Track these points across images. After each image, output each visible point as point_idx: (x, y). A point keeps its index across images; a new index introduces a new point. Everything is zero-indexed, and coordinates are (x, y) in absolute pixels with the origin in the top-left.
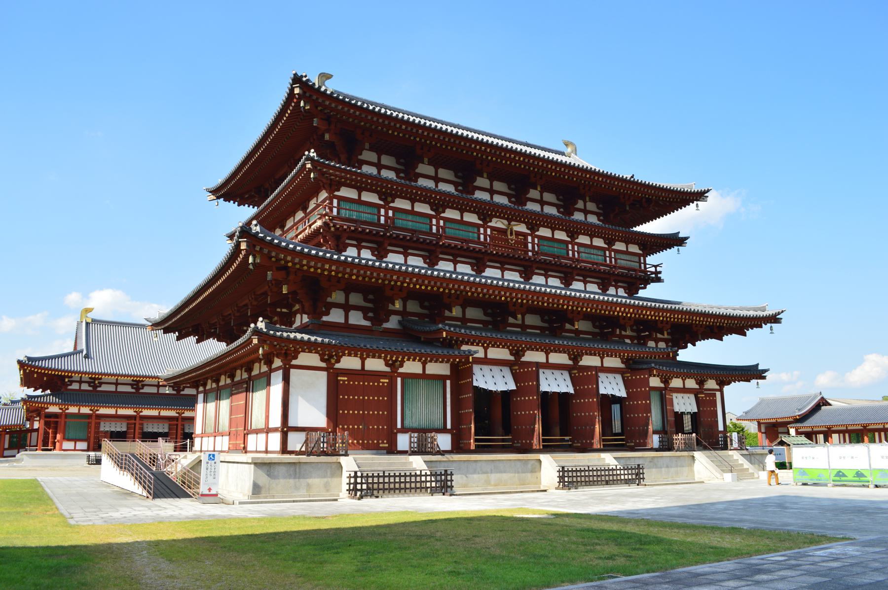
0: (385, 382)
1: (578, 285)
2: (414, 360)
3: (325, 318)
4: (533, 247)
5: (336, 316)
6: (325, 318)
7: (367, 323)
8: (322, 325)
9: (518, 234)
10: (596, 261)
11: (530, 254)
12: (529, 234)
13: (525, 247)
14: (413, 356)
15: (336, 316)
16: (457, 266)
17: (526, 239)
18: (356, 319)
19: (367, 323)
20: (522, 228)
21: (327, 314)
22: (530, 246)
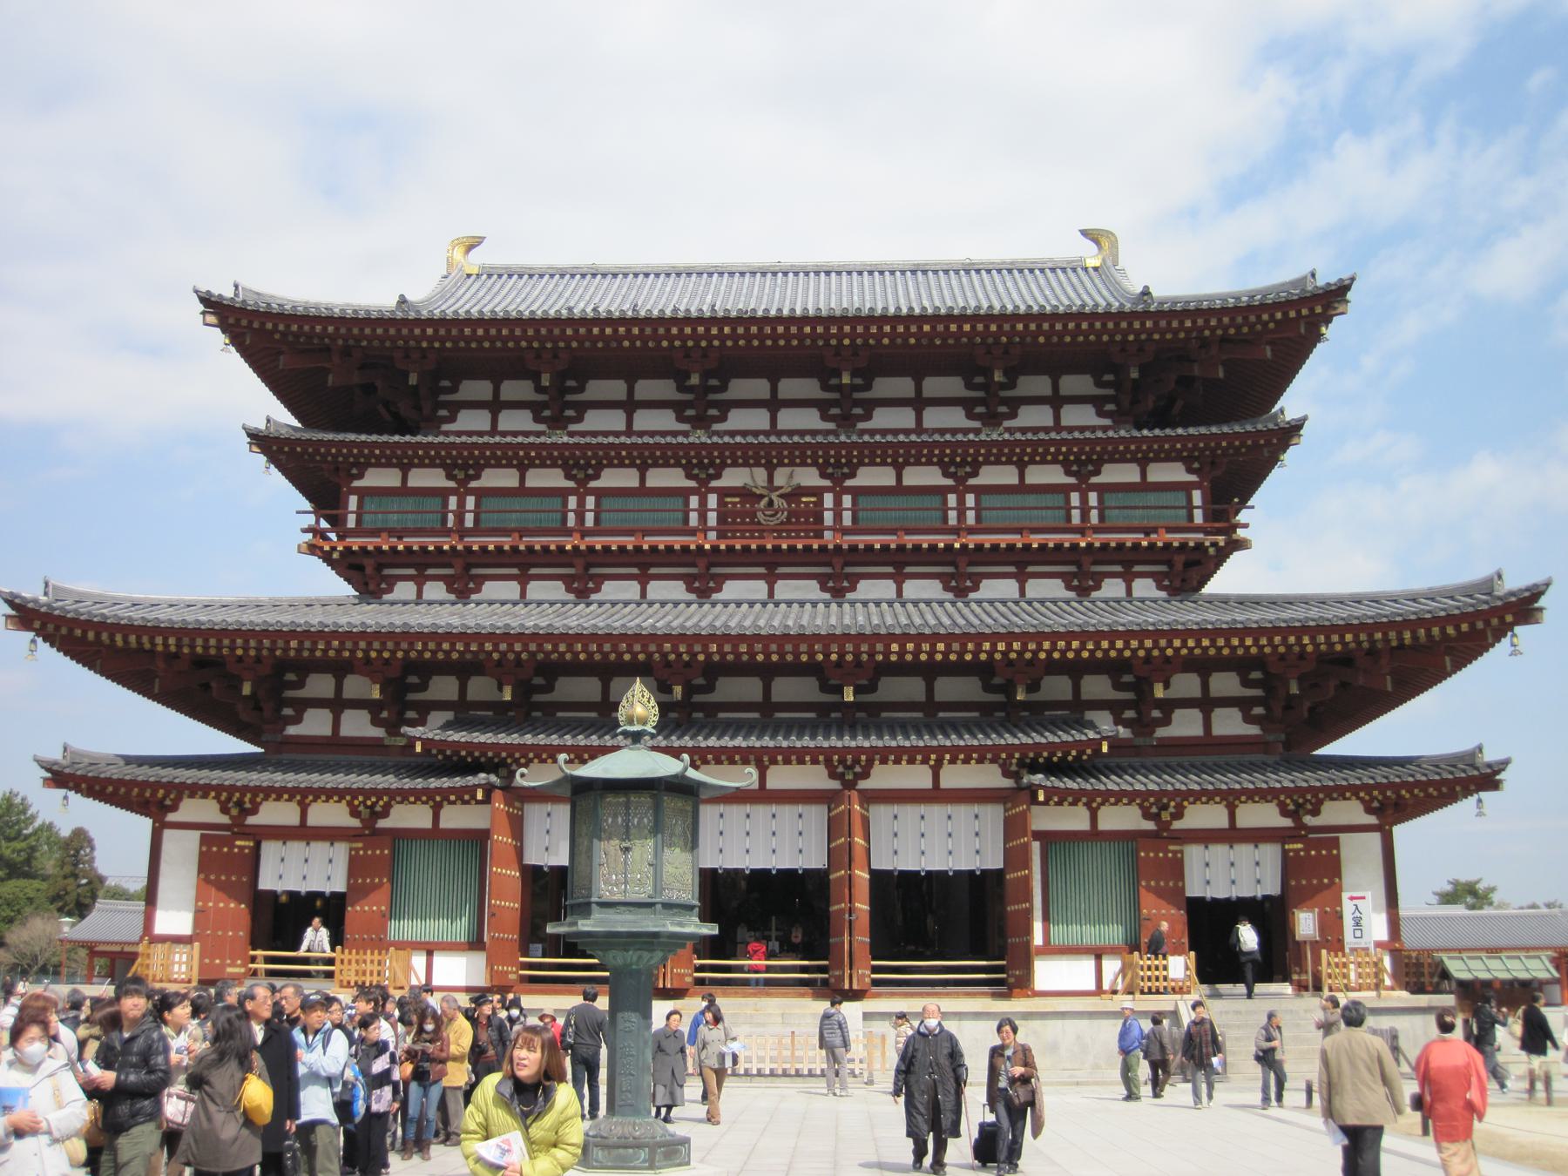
0: (245, 847)
1: (998, 589)
2: (289, 800)
3: (292, 730)
4: (838, 516)
5: (316, 724)
6: (292, 730)
7: (378, 732)
8: (281, 743)
9: (797, 493)
10: (1153, 524)
11: (828, 535)
12: (827, 489)
13: (815, 523)
14: (278, 793)
15: (316, 724)
16: (649, 587)
17: (820, 502)
18: (357, 725)
19: (378, 732)
20: (809, 477)
21: (297, 720)
22: (828, 517)
